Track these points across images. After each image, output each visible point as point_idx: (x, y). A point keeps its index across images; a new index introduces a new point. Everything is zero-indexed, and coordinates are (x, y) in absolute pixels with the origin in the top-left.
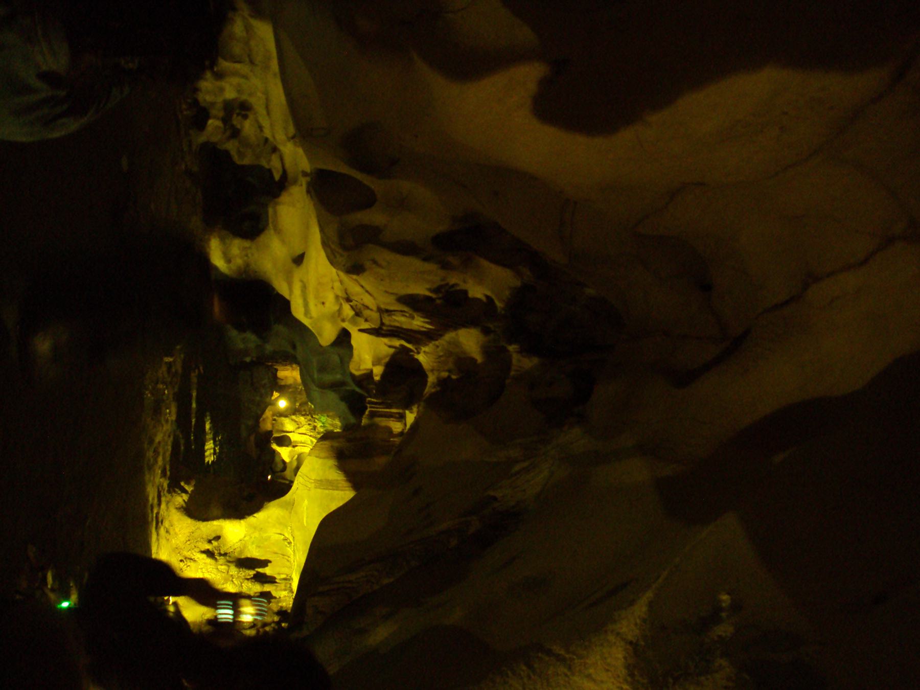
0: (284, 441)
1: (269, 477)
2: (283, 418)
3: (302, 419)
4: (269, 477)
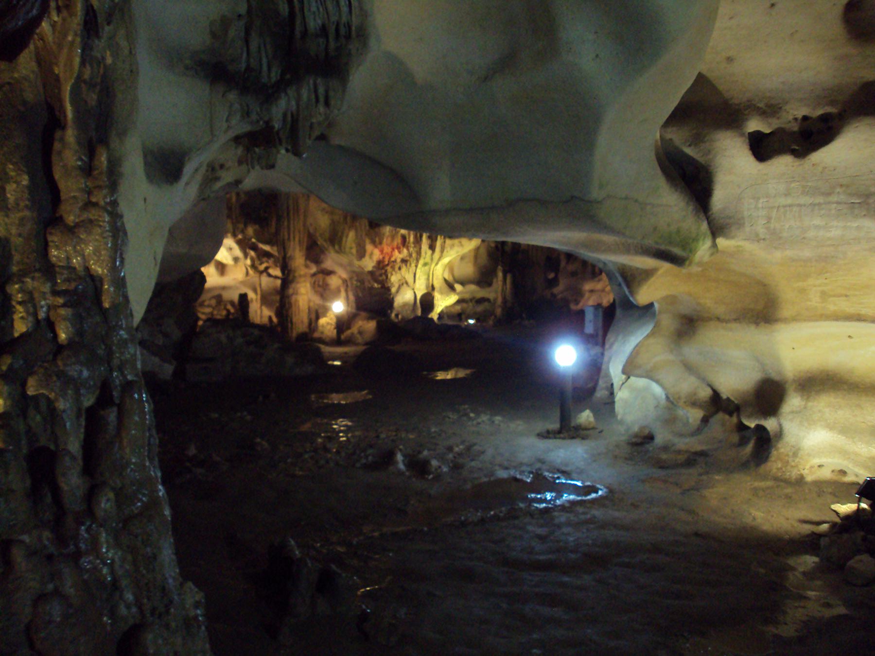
0: (427, 302)
1: (471, 322)
2: (396, 304)
3: (394, 279)
4: (471, 322)
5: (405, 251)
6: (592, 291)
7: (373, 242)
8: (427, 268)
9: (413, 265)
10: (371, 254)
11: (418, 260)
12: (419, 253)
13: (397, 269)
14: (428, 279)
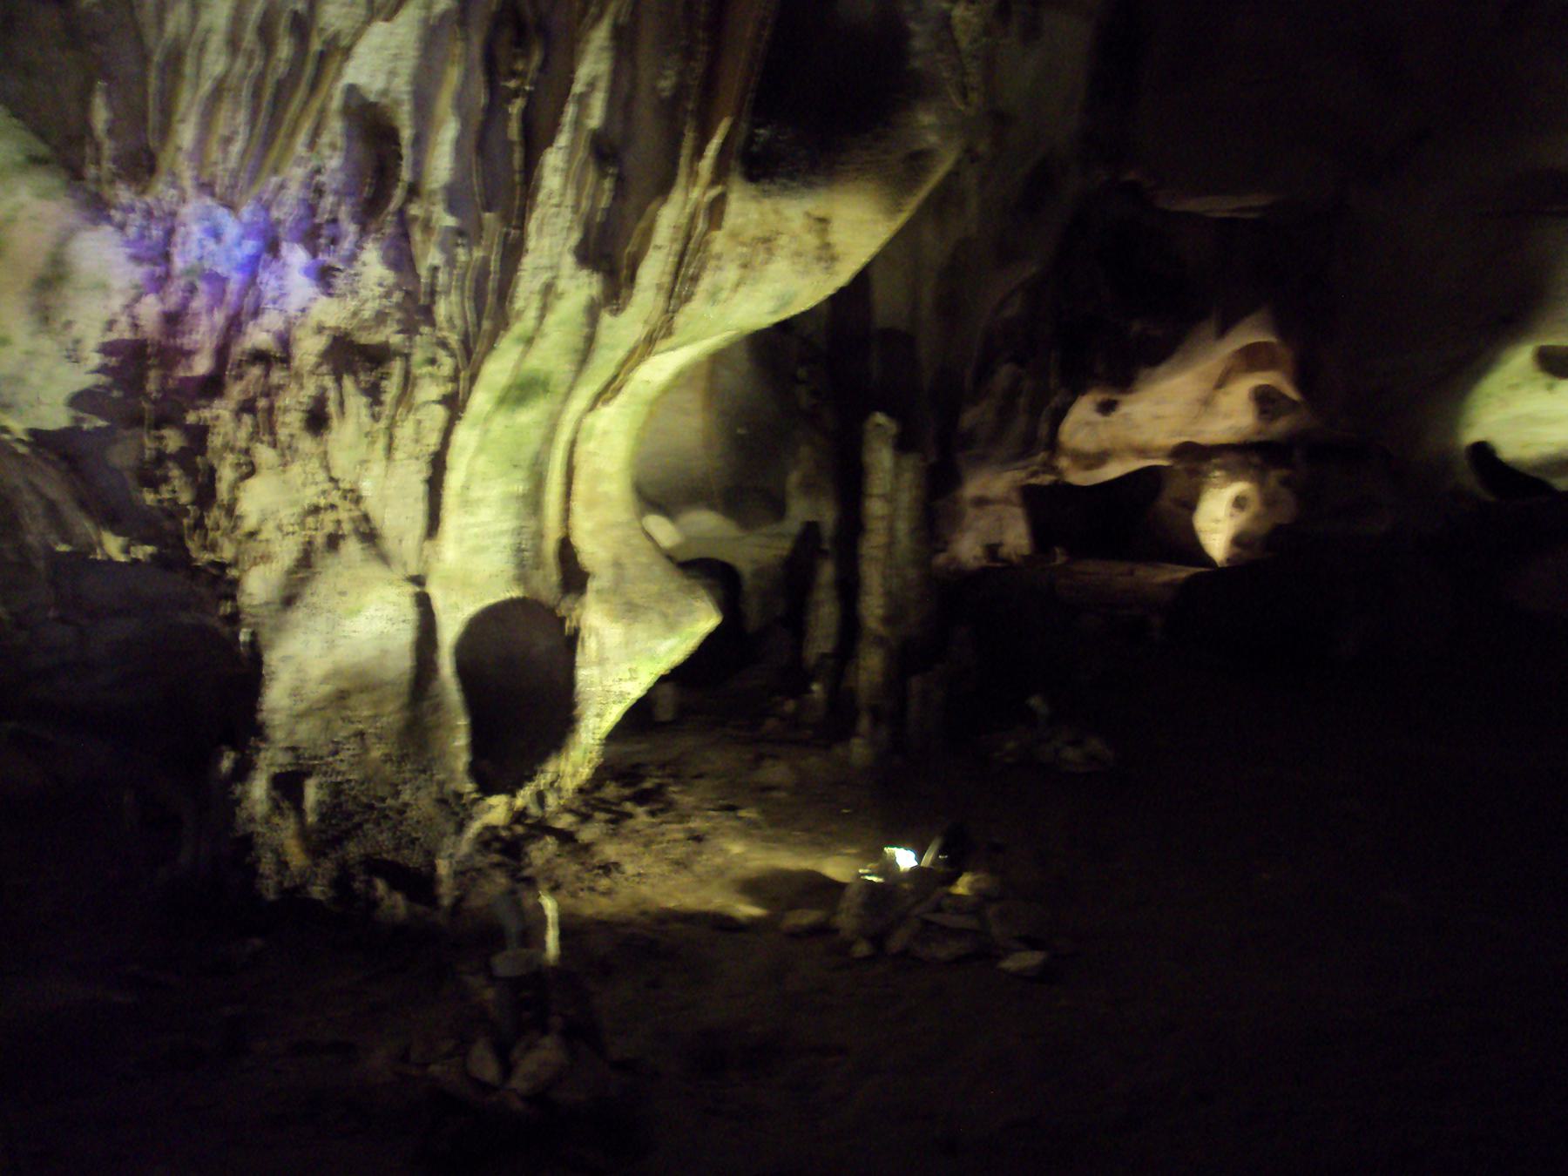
2: (277, 697)
3: (270, 501)
5: (373, 267)
6: (981, 502)
8: (530, 416)
9: (430, 391)
12: (492, 302)
13: (291, 422)
14: (533, 502)
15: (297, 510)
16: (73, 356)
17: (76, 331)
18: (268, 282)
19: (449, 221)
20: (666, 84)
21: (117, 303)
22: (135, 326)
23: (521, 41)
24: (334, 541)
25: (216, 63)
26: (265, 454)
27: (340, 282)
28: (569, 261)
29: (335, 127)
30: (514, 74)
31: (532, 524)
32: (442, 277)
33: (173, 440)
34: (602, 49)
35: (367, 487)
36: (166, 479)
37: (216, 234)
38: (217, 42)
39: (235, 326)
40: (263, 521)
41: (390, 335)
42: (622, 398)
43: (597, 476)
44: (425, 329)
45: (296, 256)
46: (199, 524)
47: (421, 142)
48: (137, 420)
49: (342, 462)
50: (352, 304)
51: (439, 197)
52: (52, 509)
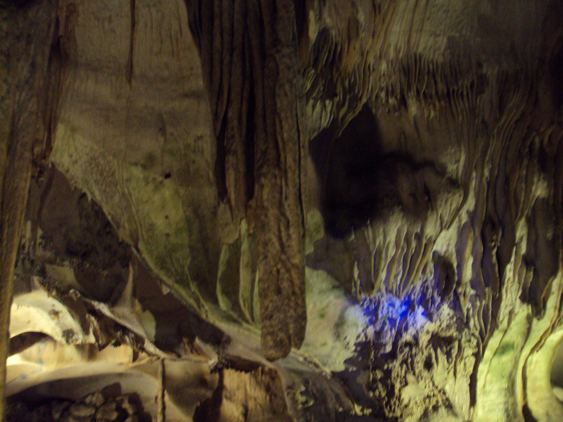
5: (446, 310)
7: (344, 286)
8: (507, 358)
9: (469, 352)
10: (340, 324)
11: (483, 339)
12: (490, 321)
13: (419, 366)
14: (511, 390)
15: (422, 397)
16: (346, 347)
17: (348, 339)
18: (410, 319)
19: (473, 292)
20: (549, 235)
21: (360, 330)
22: (366, 337)
23: (494, 228)
24: (436, 408)
25: (392, 252)
26: (410, 378)
27: (435, 317)
28: (518, 301)
29: (431, 266)
30: (492, 241)
31: (511, 400)
32: (471, 311)
33: (379, 374)
34: (522, 227)
35: (447, 388)
36: (377, 388)
37: (392, 305)
38: (392, 245)
39: (399, 334)
40: (409, 401)
41: (453, 332)
42: (543, 348)
43: (535, 379)
44: (466, 330)
45: (420, 310)
46: (388, 403)
47: (460, 266)
48: (366, 368)
49: (438, 379)
50: (438, 323)
51: (469, 284)
52: (337, 396)
